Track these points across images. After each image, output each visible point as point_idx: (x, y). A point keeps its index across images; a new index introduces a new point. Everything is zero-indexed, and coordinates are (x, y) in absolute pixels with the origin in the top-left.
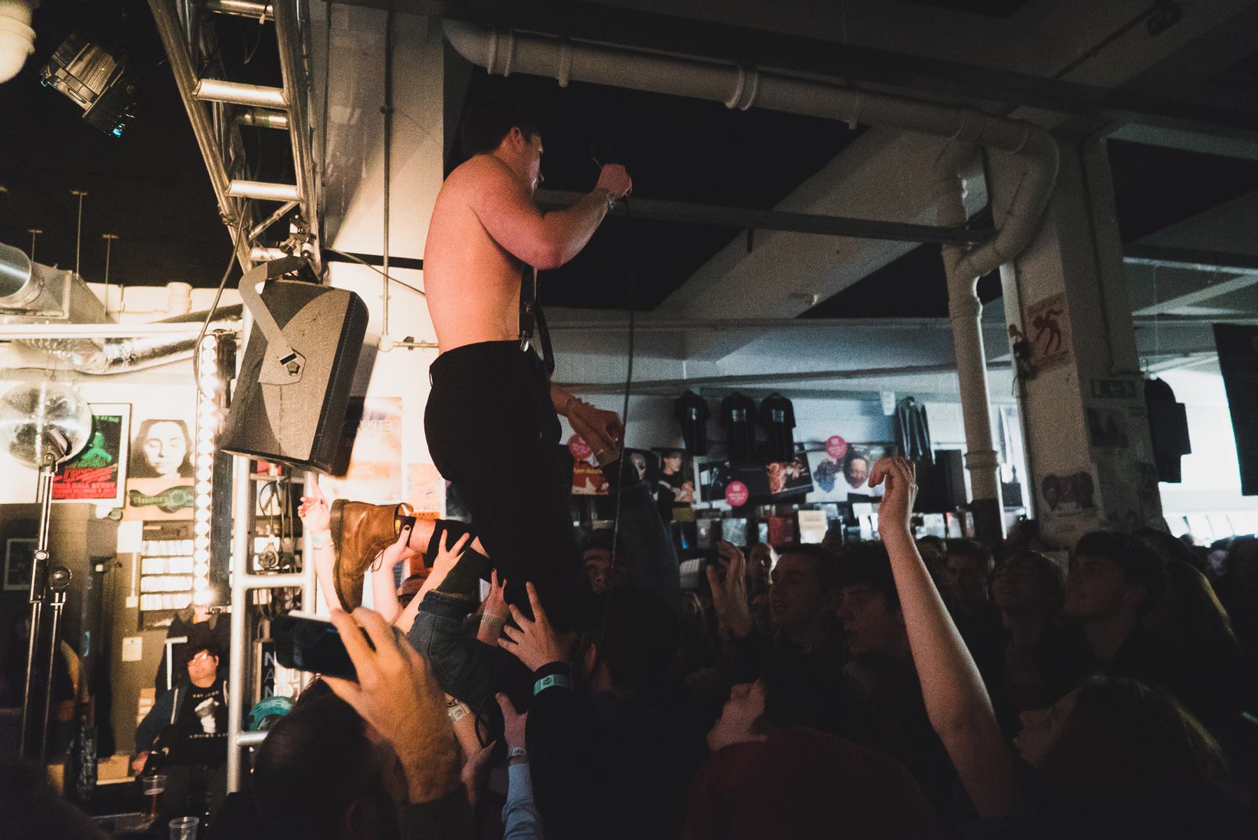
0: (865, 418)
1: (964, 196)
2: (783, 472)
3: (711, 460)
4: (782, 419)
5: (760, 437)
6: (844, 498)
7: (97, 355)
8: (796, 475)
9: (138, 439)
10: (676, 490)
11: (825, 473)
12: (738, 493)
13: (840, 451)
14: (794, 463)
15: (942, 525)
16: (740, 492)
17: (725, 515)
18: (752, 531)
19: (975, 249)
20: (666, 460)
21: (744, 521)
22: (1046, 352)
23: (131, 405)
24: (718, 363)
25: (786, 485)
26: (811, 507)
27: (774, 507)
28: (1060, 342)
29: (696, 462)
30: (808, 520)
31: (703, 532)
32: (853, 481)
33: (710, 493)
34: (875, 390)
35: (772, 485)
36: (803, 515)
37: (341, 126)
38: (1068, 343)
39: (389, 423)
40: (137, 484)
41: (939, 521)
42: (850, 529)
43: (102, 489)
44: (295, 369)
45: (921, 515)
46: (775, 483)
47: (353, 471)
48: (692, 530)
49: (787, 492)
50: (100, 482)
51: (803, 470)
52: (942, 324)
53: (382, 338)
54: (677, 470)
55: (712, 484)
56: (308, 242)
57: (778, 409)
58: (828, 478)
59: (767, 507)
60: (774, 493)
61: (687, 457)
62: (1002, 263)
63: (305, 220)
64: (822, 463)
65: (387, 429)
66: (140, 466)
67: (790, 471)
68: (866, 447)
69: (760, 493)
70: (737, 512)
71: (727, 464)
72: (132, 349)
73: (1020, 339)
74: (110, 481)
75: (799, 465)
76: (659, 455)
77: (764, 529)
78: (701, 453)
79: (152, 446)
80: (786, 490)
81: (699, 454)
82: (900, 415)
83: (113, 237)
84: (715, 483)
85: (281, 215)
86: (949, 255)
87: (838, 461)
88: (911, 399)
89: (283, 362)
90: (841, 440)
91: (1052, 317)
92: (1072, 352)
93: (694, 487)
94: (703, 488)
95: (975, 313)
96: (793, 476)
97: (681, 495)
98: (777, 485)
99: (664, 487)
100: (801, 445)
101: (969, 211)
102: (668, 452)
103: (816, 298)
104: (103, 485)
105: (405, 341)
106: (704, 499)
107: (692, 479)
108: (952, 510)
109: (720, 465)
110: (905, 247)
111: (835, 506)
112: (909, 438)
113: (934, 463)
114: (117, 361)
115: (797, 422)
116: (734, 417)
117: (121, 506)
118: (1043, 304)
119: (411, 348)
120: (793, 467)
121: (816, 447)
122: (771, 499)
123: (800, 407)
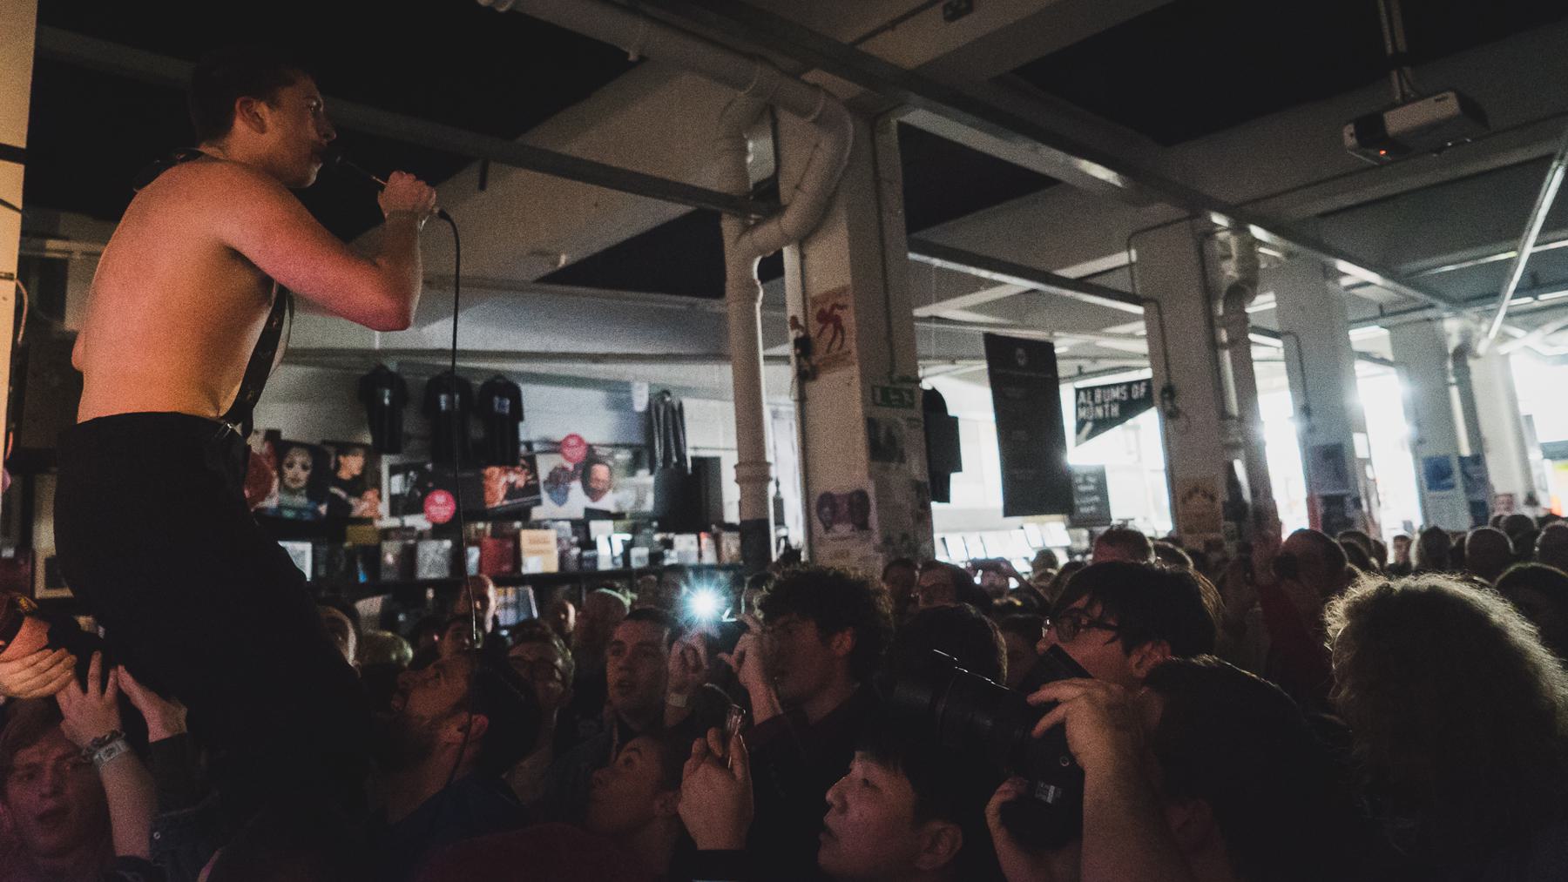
0: (614, 414)
1: (750, 159)
2: (503, 480)
3: (406, 460)
4: (507, 411)
5: (477, 432)
6: (580, 515)
8: (521, 483)
10: (353, 501)
11: (558, 481)
12: (441, 506)
13: (579, 453)
14: (519, 469)
15: (695, 548)
16: (446, 504)
17: (421, 536)
18: (457, 558)
19: (758, 223)
20: (342, 459)
21: (447, 544)
22: (828, 351)
24: (425, 330)
25: (507, 497)
26: (539, 525)
27: (489, 526)
28: (843, 340)
29: (386, 462)
30: (533, 541)
31: (390, 559)
32: (592, 492)
33: (400, 505)
34: (626, 379)
36: (526, 535)
38: (851, 344)
41: (692, 543)
42: (586, 554)
45: (671, 536)
48: (372, 555)
49: (507, 506)
51: (529, 477)
52: (715, 306)
54: (357, 472)
55: (406, 495)
57: (502, 396)
58: (561, 488)
59: (480, 525)
61: (372, 455)
62: (787, 244)
64: (556, 468)
67: (512, 477)
68: (610, 450)
69: (471, 507)
70: (438, 532)
71: (429, 466)
73: (801, 334)
75: (526, 470)
76: (331, 450)
77: (474, 554)
78: (393, 450)
80: (506, 502)
81: (390, 452)
82: (654, 413)
84: (410, 492)
86: (729, 226)
87: (575, 467)
88: (668, 393)
90: (580, 440)
91: (837, 312)
92: (854, 352)
93: (380, 497)
94: (394, 499)
95: (755, 299)
96: (517, 486)
97: (361, 507)
98: (494, 494)
99: (336, 496)
100: (529, 445)
101: (755, 176)
102: (345, 448)
106: (394, 512)
107: (378, 485)
108: (707, 529)
109: (419, 468)
110: (676, 210)
111: (567, 525)
112: (662, 441)
113: (690, 471)
115: (526, 414)
116: (443, 405)
118: (827, 296)
120: (516, 472)
121: (547, 447)
122: (485, 515)
123: (531, 394)
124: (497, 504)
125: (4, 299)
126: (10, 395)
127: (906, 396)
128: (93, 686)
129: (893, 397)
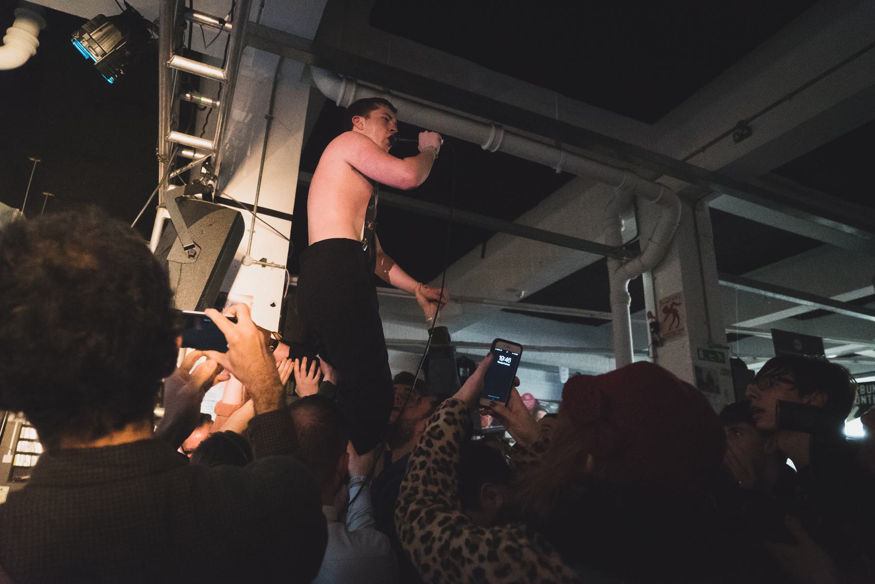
0: (547, 383)
1: (623, 229)
19: (627, 261)
22: (670, 329)
25: (492, 424)
35: (483, 422)
37: (238, 122)
38: (684, 324)
44: (192, 254)
46: (485, 422)
53: (246, 257)
56: (212, 180)
60: (483, 428)
62: (644, 271)
63: (213, 166)
68: (547, 403)
73: (654, 320)
80: (491, 427)
83: (50, 194)
85: (193, 165)
86: (612, 264)
89: (186, 249)
91: (674, 307)
92: (686, 329)
95: (627, 303)
103: (523, 293)
105: (261, 260)
118: (669, 299)
119: (264, 266)
124: (487, 427)
126: (280, 319)
127: (719, 355)
128: (311, 374)
129: (710, 356)
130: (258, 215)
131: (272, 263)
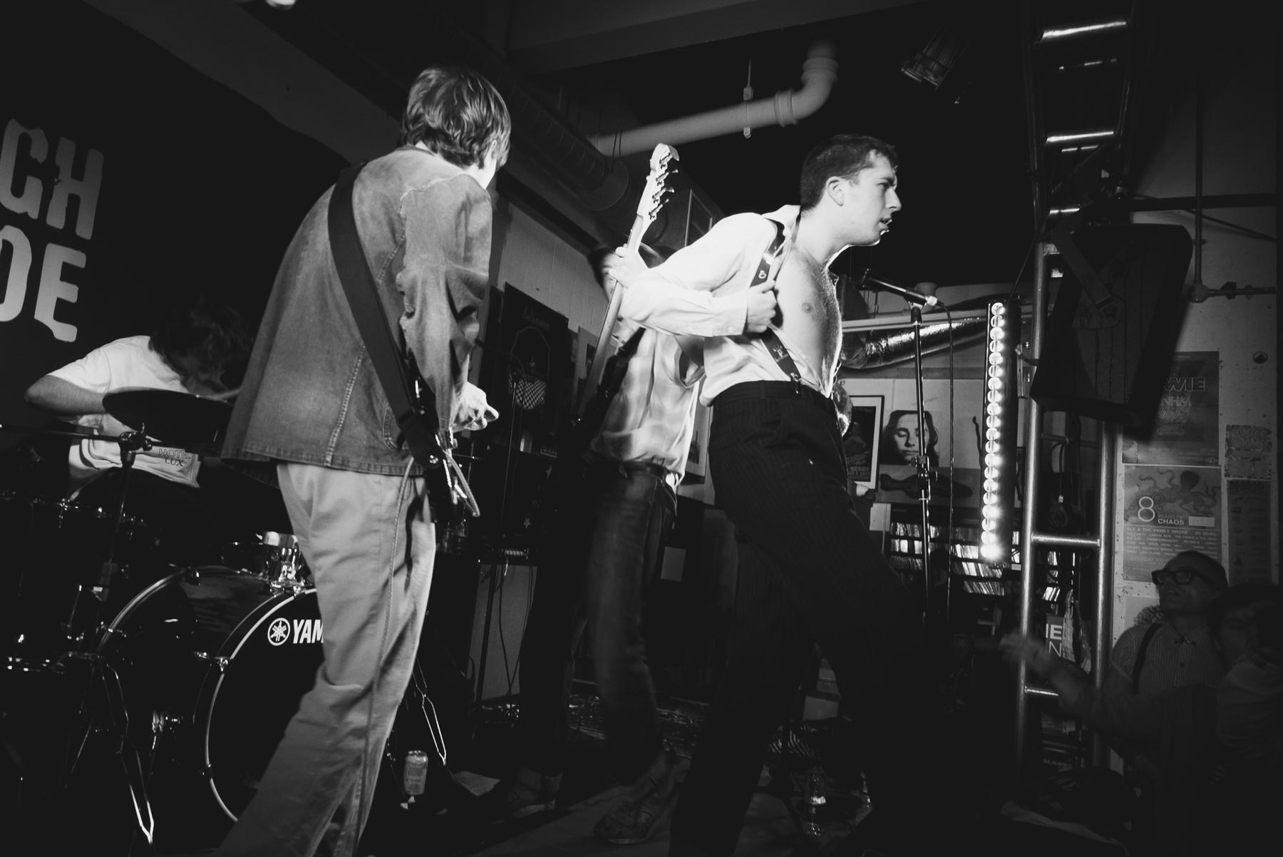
7: (859, 352)
9: (888, 427)
23: (883, 397)
39: (1202, 380)
40: (887, 470)
43: (859, 473)
47: (1161, 431)
50: (858, 466)
65: (1200, 387)
66: (891, 454)
72: (887, 344)
74: (862, 466)
79: (900, 436)
104: (859, 468)
105: (1223, 288)
114: (874, 358)
117: (874, 487)
125: (1269, 308)
130: (1206, 212)
131: (1248, 287)
